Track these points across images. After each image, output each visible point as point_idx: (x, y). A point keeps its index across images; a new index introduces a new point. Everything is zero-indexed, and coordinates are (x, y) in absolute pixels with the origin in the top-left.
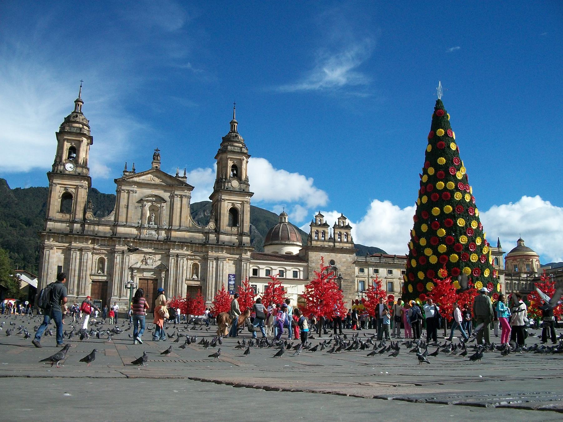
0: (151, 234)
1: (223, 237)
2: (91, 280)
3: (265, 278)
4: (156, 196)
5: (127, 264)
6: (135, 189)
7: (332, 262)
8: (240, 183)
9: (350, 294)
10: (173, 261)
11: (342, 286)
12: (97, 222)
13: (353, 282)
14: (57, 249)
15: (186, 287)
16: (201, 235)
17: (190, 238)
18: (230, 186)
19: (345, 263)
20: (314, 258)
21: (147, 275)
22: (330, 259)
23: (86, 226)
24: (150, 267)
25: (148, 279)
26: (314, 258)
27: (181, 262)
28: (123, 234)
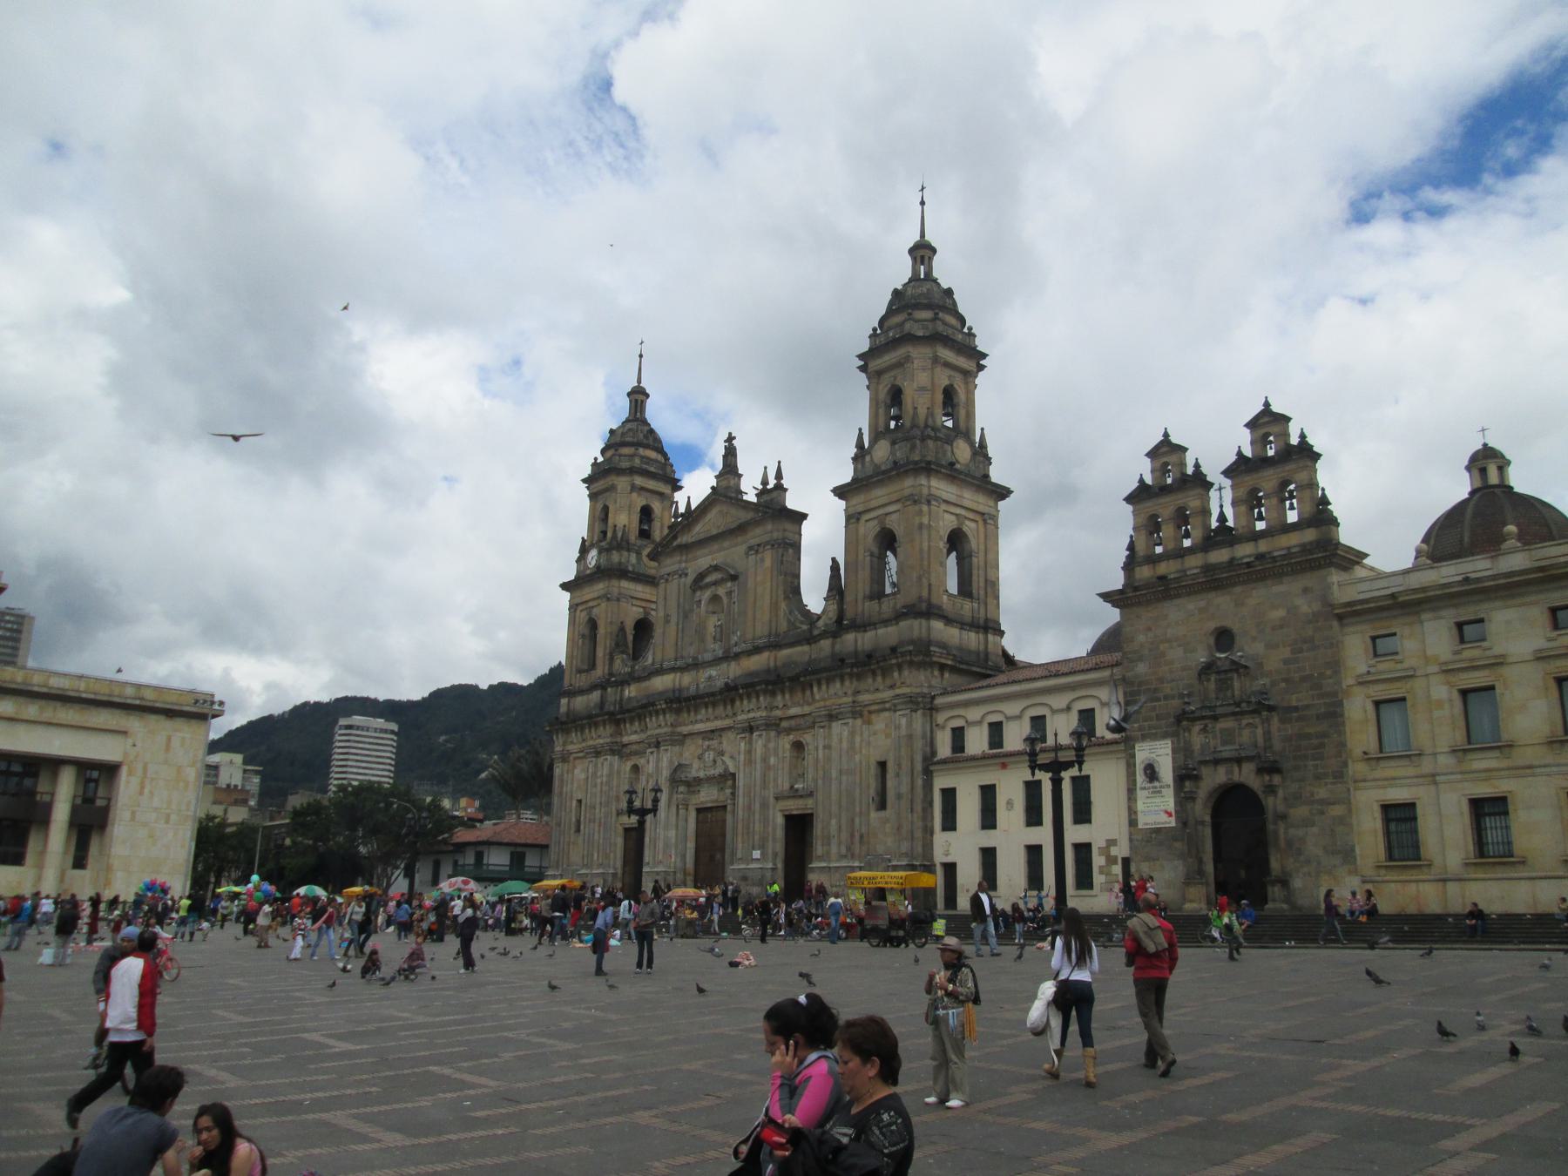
0: (710, 677)
1: (851, 641)
2: (620, 831)
3: (984, 757)
4: (716, 568)
6: (683, 565)
7: (1224, 638)
8: (893, 443)
9: (1318, 777)
10: (742, 744)
11: (1277, 745)
13: (1334, 714)
14: (575, 759)
15: (780, 820)
16: (806, 648)
18: (867, 464)
19: (1281, 627)
20: (1141, 638)
21: (707, 796)
22: (1212, 625)
23: (609, 690)
24: (712, 772)
25: (710, 809)
26: (1141, 638)
27: (759, 745)
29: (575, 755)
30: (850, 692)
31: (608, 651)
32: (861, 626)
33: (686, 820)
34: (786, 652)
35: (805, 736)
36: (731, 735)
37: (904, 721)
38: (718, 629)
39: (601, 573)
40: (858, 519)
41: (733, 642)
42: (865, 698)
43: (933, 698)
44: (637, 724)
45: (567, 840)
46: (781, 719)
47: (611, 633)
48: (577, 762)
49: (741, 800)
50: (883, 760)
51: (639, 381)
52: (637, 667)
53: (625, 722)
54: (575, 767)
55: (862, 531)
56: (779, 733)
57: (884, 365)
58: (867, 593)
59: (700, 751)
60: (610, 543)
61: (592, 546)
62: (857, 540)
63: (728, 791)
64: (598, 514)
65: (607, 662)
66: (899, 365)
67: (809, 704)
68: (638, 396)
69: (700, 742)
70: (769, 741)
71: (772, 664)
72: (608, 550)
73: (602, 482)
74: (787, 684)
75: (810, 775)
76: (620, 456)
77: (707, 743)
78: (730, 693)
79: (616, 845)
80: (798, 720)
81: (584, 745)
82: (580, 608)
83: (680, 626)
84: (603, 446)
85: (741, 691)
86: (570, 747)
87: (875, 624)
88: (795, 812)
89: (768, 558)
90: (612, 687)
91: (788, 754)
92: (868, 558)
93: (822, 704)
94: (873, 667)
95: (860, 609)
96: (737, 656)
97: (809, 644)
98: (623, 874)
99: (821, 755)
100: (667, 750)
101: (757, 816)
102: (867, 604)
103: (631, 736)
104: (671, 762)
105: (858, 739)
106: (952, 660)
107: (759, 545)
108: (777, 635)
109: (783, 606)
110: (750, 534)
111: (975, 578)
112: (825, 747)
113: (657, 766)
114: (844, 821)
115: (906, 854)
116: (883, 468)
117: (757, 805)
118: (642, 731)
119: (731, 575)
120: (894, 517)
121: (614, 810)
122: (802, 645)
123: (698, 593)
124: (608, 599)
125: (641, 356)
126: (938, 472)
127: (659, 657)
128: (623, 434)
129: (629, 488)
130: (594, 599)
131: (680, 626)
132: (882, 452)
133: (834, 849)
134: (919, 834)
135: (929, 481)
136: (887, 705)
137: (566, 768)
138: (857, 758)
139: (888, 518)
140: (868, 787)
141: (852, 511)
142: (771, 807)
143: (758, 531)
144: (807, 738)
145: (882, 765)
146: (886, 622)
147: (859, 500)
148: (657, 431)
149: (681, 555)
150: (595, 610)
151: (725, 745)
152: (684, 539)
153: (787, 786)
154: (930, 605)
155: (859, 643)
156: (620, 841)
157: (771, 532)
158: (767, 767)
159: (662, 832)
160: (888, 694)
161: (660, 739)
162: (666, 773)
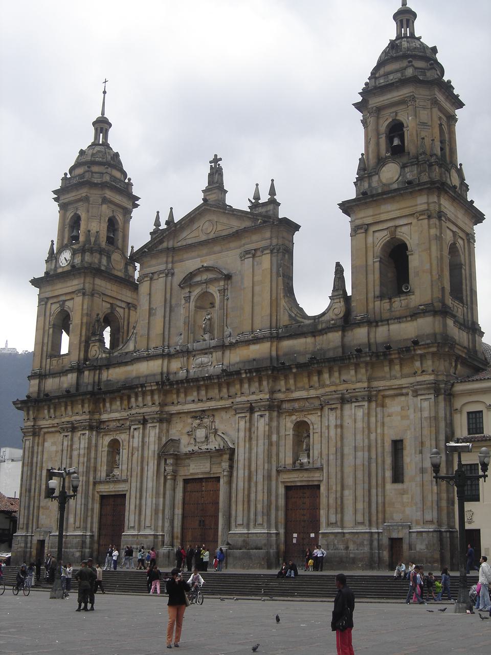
0: (202, 365)
1: (360, 335)
2: (98, 496)
4: (207, 269)
5: (152, 447)
8: (403, 167)
10: (242, 423)
12: (105, 362)
14: (45, 433)
15: (282, 491)
16: (310, 340)
17: (285, 355)
18: (374, 184)
21: (196, 468)
23: (86, 373)
24: (204, 447)
28: (147, 376)
29: (46, 430)
30: (365, 378)
31: (83, 338)
32: (372, 322)
33: (174, 490)
34: (287, 344)
35: (310, 417)
36: (223, 414)
37: (426, 404)
38: (208, 322)
39: (73, 271)
40: (366, 231)
41: (227, 333)
42: (375, 384)
43: (453, 385)
44: (118, 403)
45: (36, 504)
46: (282, 401)
47: (87, 323)
48: (47, 436)
49: (241, 472)
50: (398, 438)
51: (103, 113)
52: (116, 354)
53: (104, 401)
54: (44, 441)
55: (370, 240)
56: (278, 412)
57: (387, 102)
58: (377, 293)
59: (188, 429)
60: (84, 246)
61: (62, 248)
62: (366, 248)
63: (225, 465)
64: (68, 221)
65: (83, 349)
66: (402, 102)
67: (316, 389)
68: (102, 125)
69: (190, 420)
70: (271, 419)
71: (274, 353)
72: (83, 251)
73: (73, 194)
74: (294, 370)
75: (315, 452)
76: (92, 173)
77: (198, 421)
78: (229, 377)
79: (92, 510)
80: (302, 403)
81: (56, 421)
82: (51, 301)
83: (167, 319)
84: (72, 163)
85: (244, 376)
86: (42, 423)
87: (388, 320)
88: (299, 484)
89: (266, 261)
90: (89, 370)
91: (291, 432)
92: (378, 263)
93: (333, 388)
94: (393, 357)
95: (371, 306)
96: (232, 346)
97: (314, 336)
98: (99, 535)
99: (332, 432)
100: (155, 427)
101: (260, 487)
102: (378, 303)
103: (112, 413)
104: (160, 438)
105: (373, 420)
106: (466, 353)
107: (255, 250)
108: (277, 328)
109: (283, 303)
110: (243, 242)
111: (464, 287)
112: (336, 426)
113: (143, 442)
114: (360, 493)
115: (432, 522)
116: (395, 186)
117: (260, 477)
118: (129, 408)
119: (225, 275)
120: (404, 229)
121: (91, 479)
122: (305, 337)
123: (187, 290)
124: (84, 294)
125: (105, 92)
126: (447, 192)
127: (142, 346)
128: (93, 155)
129: (100, 200)
130: (66, 294)
131: (167, 319)
132: (390, 173)
133: (349, 517)
134: (444, 504)
135: (439, 200)
136: (404, 391)
137: (36, 441)
138: (373, 436)
139: (399, 230)
140: (384, 462)
141: (358, 222)
142: (274, 478)
143: (255, 238)
144: (313, 419)
145: (398, 446)
146: (399, 319)
147: (366, 215)
148: (122, 158)
149: (167, 257)
150: (67, 303)
151: (218, 424)
152: (170, 244)
153: (289, 460)
154: (444, 304)
155: (372, 336)
156: (97, 506)
157: (271, 238)
158: (271, 444)
159: (149, 500)
160: (404, 382)
161: (146, 417)
162: (153, 447)
